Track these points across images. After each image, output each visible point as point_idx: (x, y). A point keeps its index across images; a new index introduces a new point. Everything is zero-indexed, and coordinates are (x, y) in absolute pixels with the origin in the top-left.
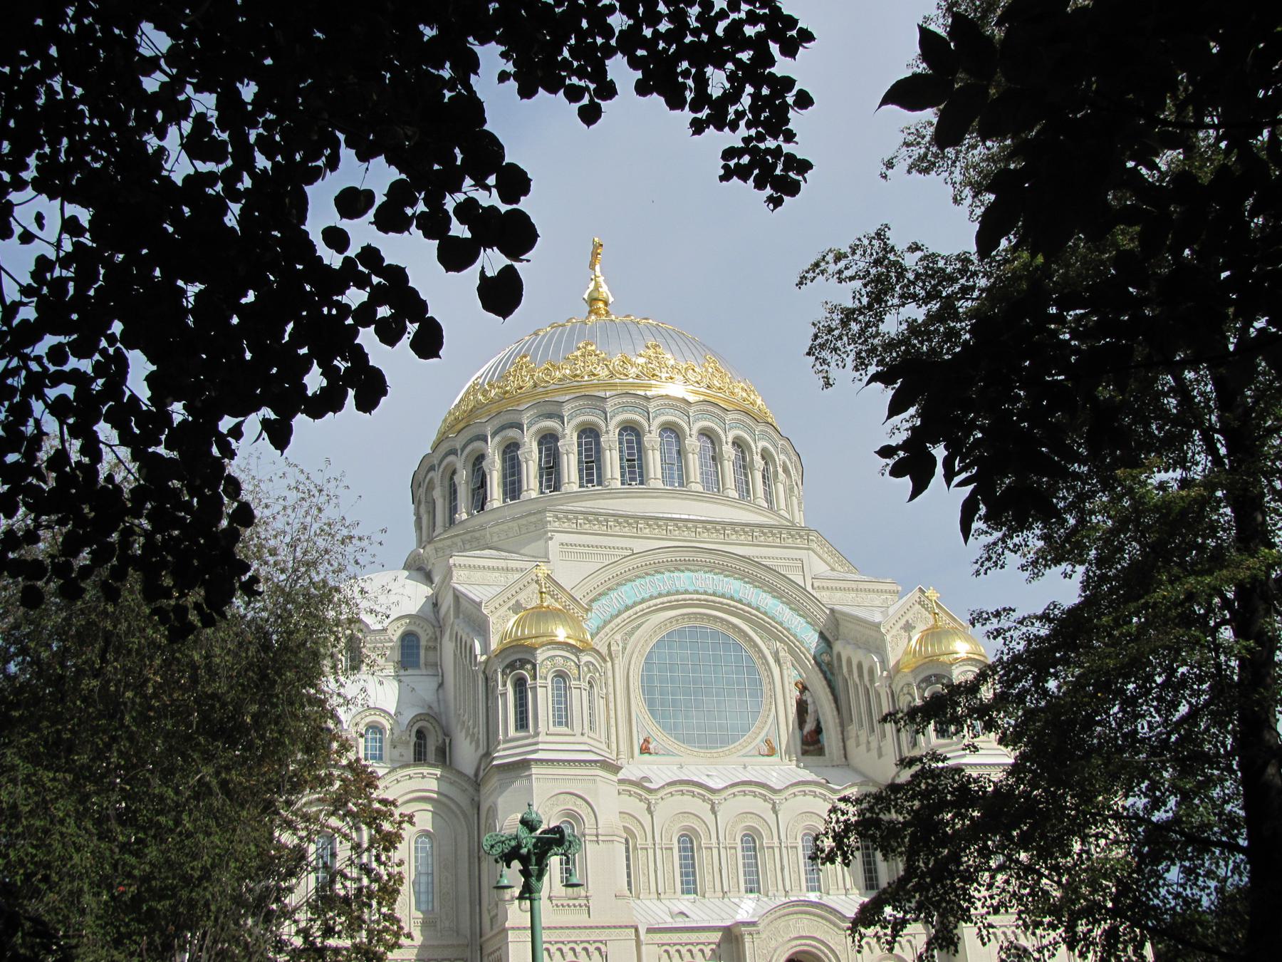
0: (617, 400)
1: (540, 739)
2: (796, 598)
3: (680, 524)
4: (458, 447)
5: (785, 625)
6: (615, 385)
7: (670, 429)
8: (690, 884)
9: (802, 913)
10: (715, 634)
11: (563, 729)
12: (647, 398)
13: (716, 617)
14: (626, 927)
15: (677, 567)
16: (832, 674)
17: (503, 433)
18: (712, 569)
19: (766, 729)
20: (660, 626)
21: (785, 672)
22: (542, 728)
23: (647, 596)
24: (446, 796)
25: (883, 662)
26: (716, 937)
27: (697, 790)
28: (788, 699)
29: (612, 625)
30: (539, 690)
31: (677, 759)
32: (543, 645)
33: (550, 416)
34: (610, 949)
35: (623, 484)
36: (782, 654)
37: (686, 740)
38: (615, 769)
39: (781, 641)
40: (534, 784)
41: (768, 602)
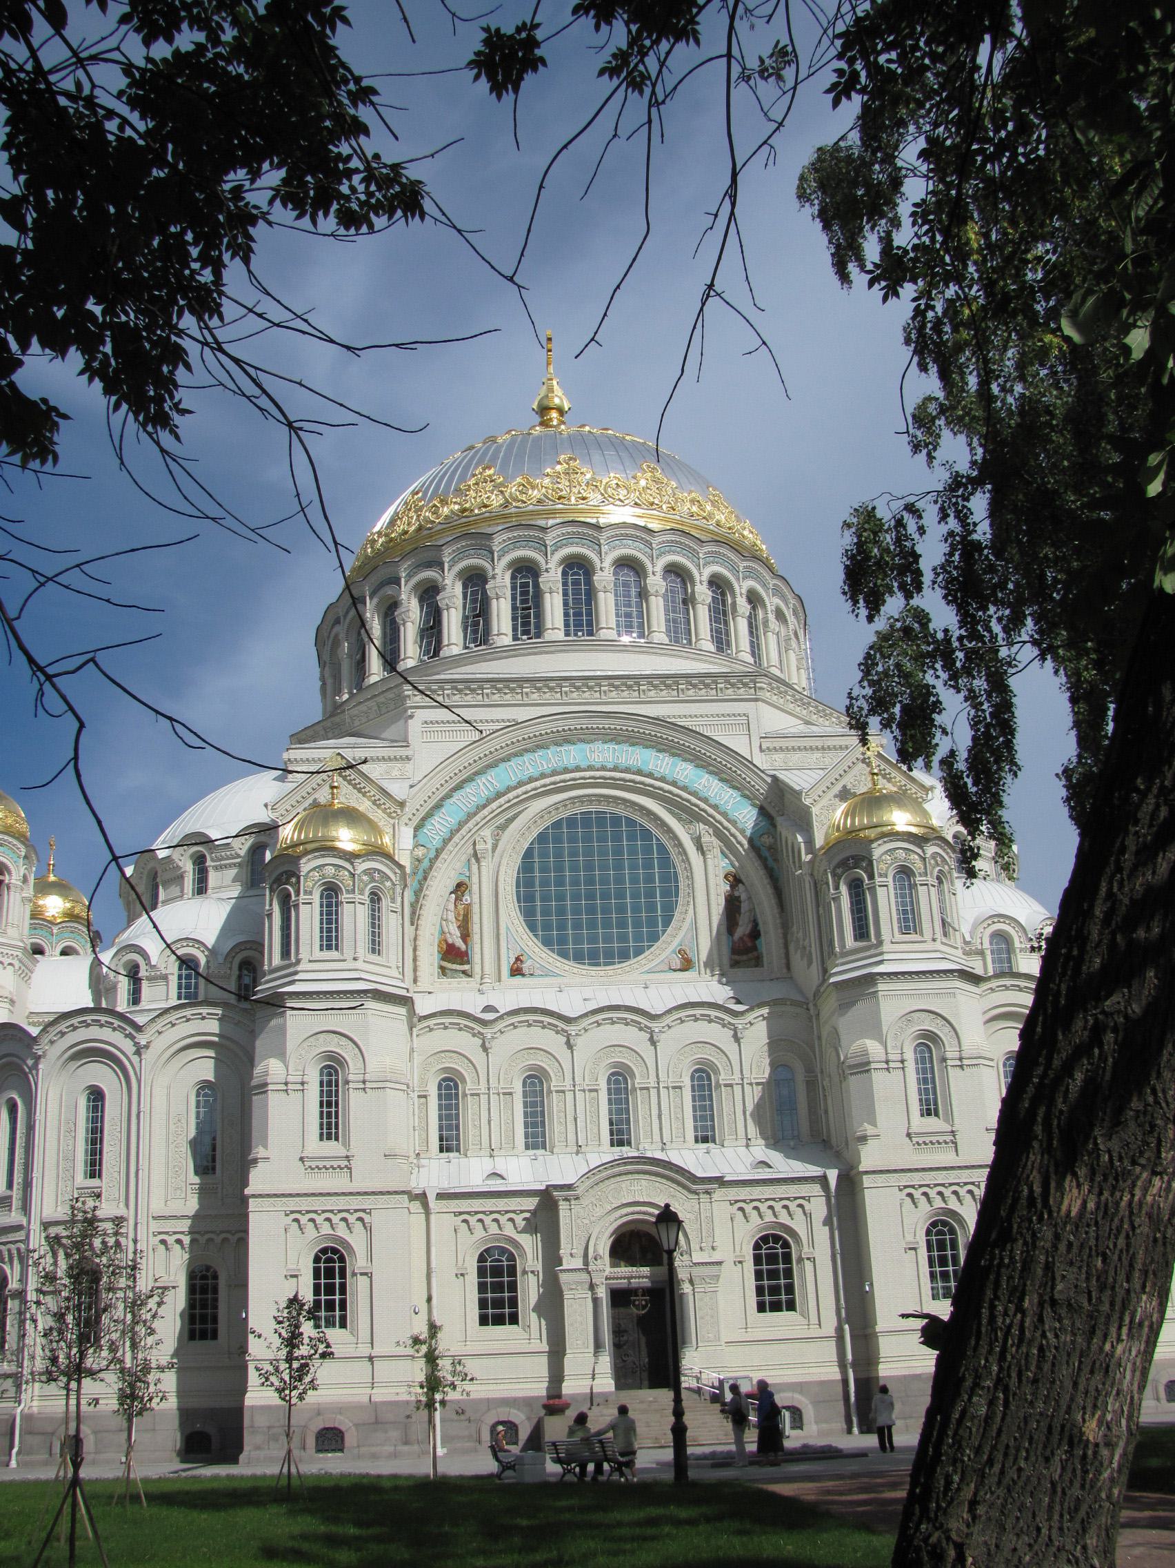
0: (505, 537)
1: (299, 968)
2: (725, 766)
3: (579, 684)
4: (341, 614)
5: (712, 801)
6: (505, 516)
7: (627, 564)
8: (537, 1137)
9: (638, 1172)
10: (616, 820)
11: (334, 954)
12: (597, 527)
13: (616, 798)
14: (396, 1193)
15: (566, 739)
16: (776, 860)
17: (381, 592)
19: (681, 934)
20: (541, 815)
21: (709, 862)
22: (304, 955)
23: (525, 778)
24: (228, 1038)
25: (810, 842)
26: (531, 1203)
27: (547, 1019)
28: (713, 897)
29: (477, 818)
30: (302, 907)
31: (559, 980)
32: (306, 853)
33: (429, 565)
35: (567, 634)
36: (705, 839)
37: (578, 957)
38: (405, 1001)
39: (706, 822)
40: (289, 1023)
41: (684, 771)
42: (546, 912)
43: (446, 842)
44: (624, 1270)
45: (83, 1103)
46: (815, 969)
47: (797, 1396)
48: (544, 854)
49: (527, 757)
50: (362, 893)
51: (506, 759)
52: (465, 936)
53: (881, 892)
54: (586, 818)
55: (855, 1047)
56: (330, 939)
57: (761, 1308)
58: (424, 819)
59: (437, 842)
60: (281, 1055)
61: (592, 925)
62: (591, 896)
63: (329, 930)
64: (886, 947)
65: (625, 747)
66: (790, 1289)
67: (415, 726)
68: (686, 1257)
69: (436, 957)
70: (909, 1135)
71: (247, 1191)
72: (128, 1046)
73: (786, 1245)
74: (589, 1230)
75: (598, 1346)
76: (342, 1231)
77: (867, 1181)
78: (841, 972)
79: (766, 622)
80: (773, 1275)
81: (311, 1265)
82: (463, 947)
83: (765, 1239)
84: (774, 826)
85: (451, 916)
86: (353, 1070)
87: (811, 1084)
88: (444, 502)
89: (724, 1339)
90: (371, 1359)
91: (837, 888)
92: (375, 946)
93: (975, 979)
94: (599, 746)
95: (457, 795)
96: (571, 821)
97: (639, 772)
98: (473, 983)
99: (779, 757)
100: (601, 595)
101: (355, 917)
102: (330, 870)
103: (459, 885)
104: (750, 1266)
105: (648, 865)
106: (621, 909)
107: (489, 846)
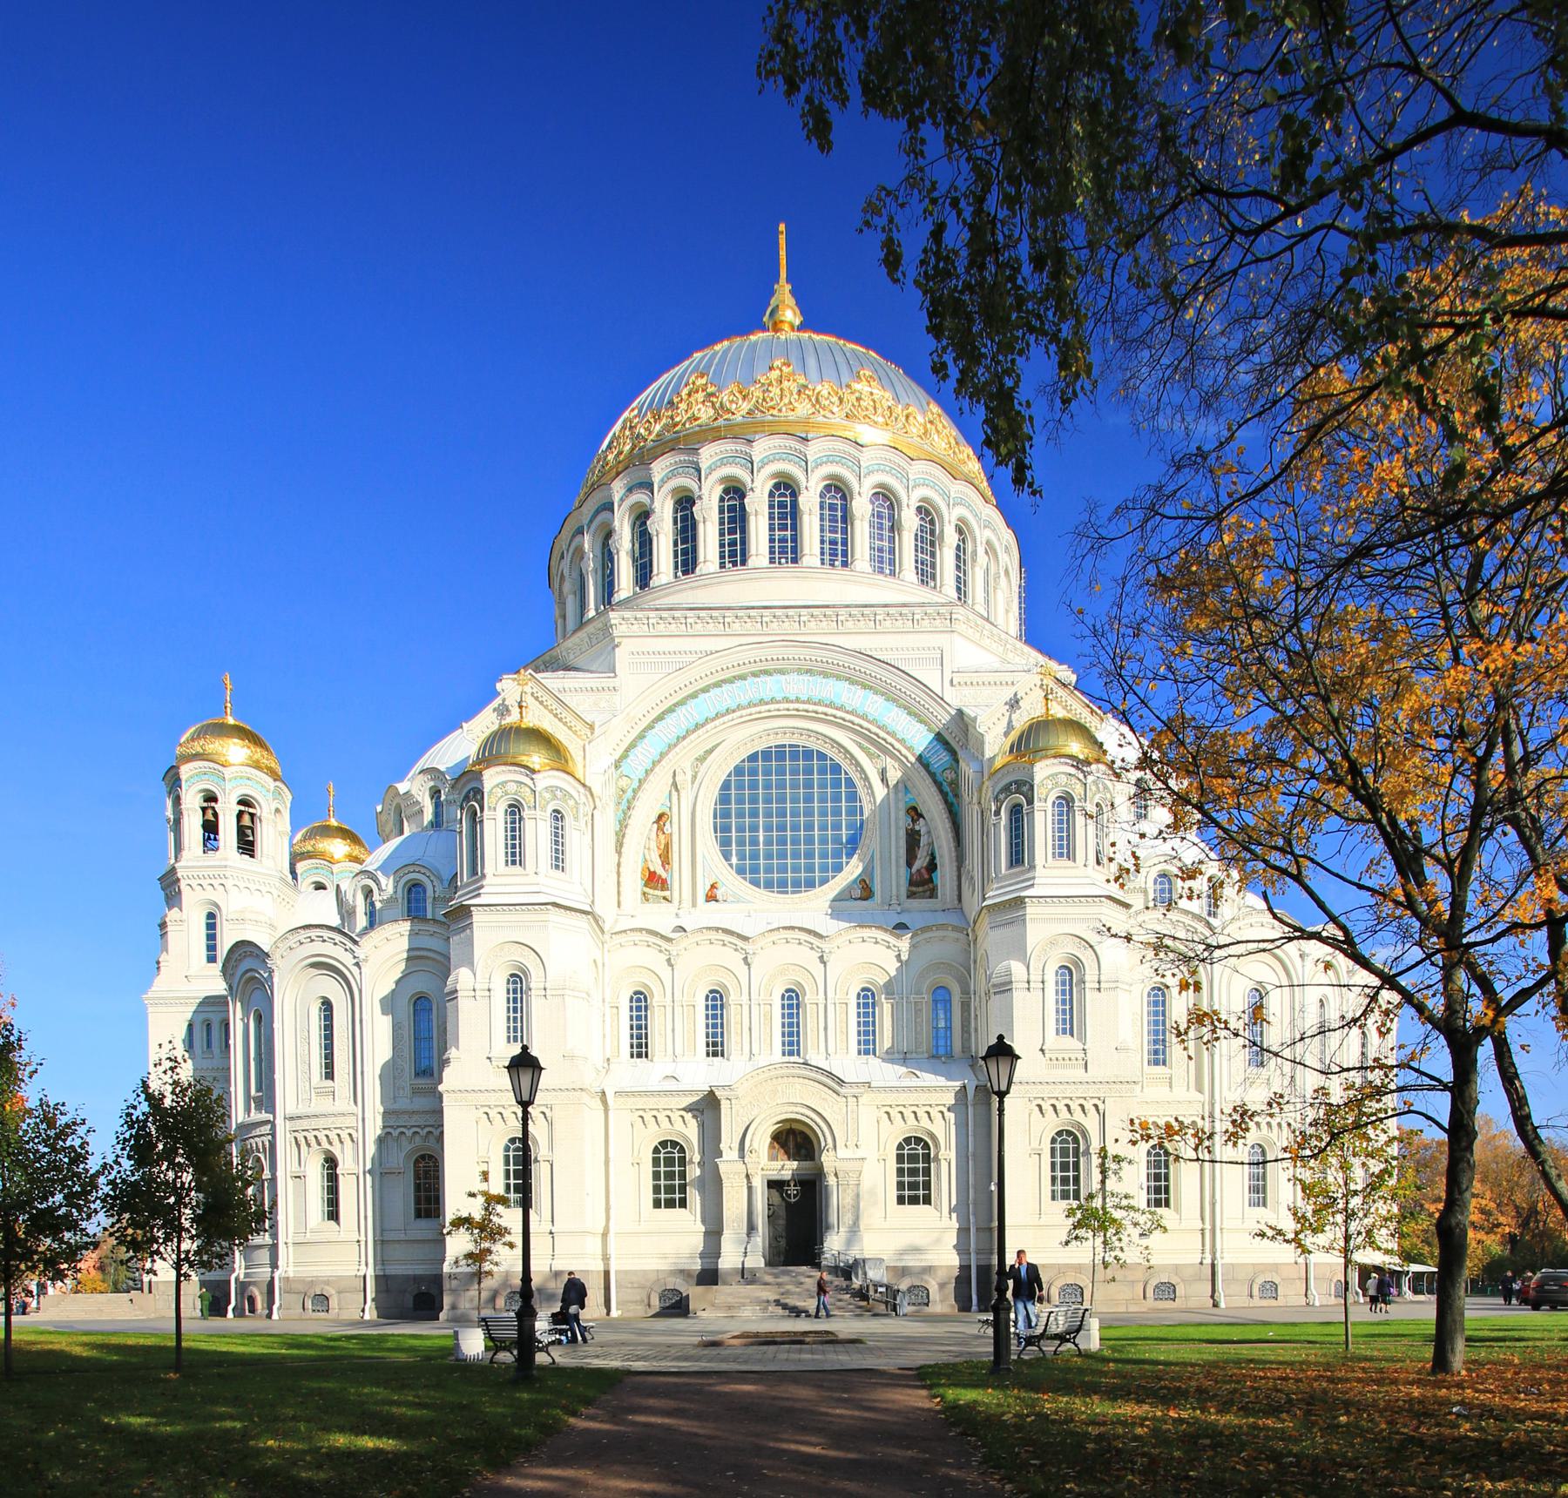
8: (715, 1048)
10: (808, 754)
51: (705, 690)
52: (665, 859)
55: (1000, 968)
68: (832, 1153)
71: (440, 1088)
72: (348, 960)
79: (975, 552)
80: (913, 1172)
83: (908, 1140)
86: (535, 982)
95: (659, 726)
96: (767, 755)
99: (967, 691)
105: (836, 798)
107: (689, 774)
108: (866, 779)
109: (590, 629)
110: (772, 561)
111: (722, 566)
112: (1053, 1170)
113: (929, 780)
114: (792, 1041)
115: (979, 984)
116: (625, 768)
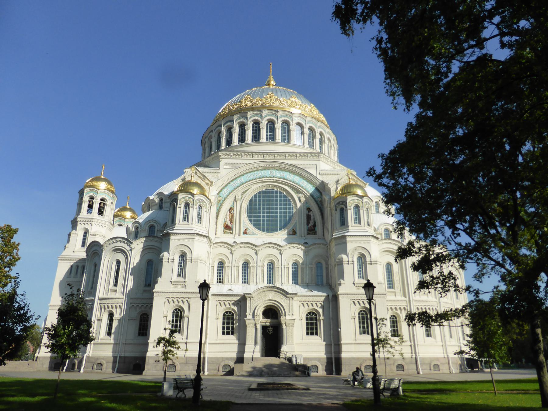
8: (245, 280)
10: (277, 192)
11: (186, 222)
16: (322, 205)
18: (278, 169)
22: (177, 222)
34: (192, 301)
37: (263, 230)
41: (297, 179)
42: (255, 217)
43: (227, 196)
44: (266, 320)
45: (114, 264)
46: (330, 235)
47: (316, 362)
48: (255, 200)
49: (252, 173)
50: (196, 205)
51: (246, 174)
53: (349, 212)
54: (268, 191)
56: (186, 218)
57: (307, 334)
58: (222, 189)
59: (225, 196)
60: (168, 250)
61: (268, 221)
62: (268, 213)
63: (185, 216)
64: (350, 227)
65: (280, 172)
66: (316, 329)
67: (222, 164)
68: (284, 317)
69: (223, 228)
70: (354, 284)
71: (154, 291)
72: (128, 248)
73: (316, 315)
74: (256, 308)
75: (256, 343)
76: (181, 304)
77: (340, 297)
78: (336, 235)
79: (324, 140)
80: (312, 324)
81: (171, 314)
82: (231, 226)
84: (322, 195)
85: (228, 217)
87: (327, 269)
88: (236, 104)
89: (295, 343)
90: (186, 343)
91: (336, 210)
92: (199, 221)
93: (377, 238)
94: (273, 171)
95: (231, 183)
97: (284, 179)
98: (232, 236)
99: (324, 176)
100: (277, 130)
101: (194, 212)
102: (187, 198)
103: (231, 208)
104: (304, 321)
105: (285, 205)
106: (276, 217)
108: (294, 200)
109: (213, 156)
110: (267, 140)
111: (252, 141)
112: (360, 324)
113: (313, 200)
114: (271, 279)
115: (332, 262)
116: (220, 194)
